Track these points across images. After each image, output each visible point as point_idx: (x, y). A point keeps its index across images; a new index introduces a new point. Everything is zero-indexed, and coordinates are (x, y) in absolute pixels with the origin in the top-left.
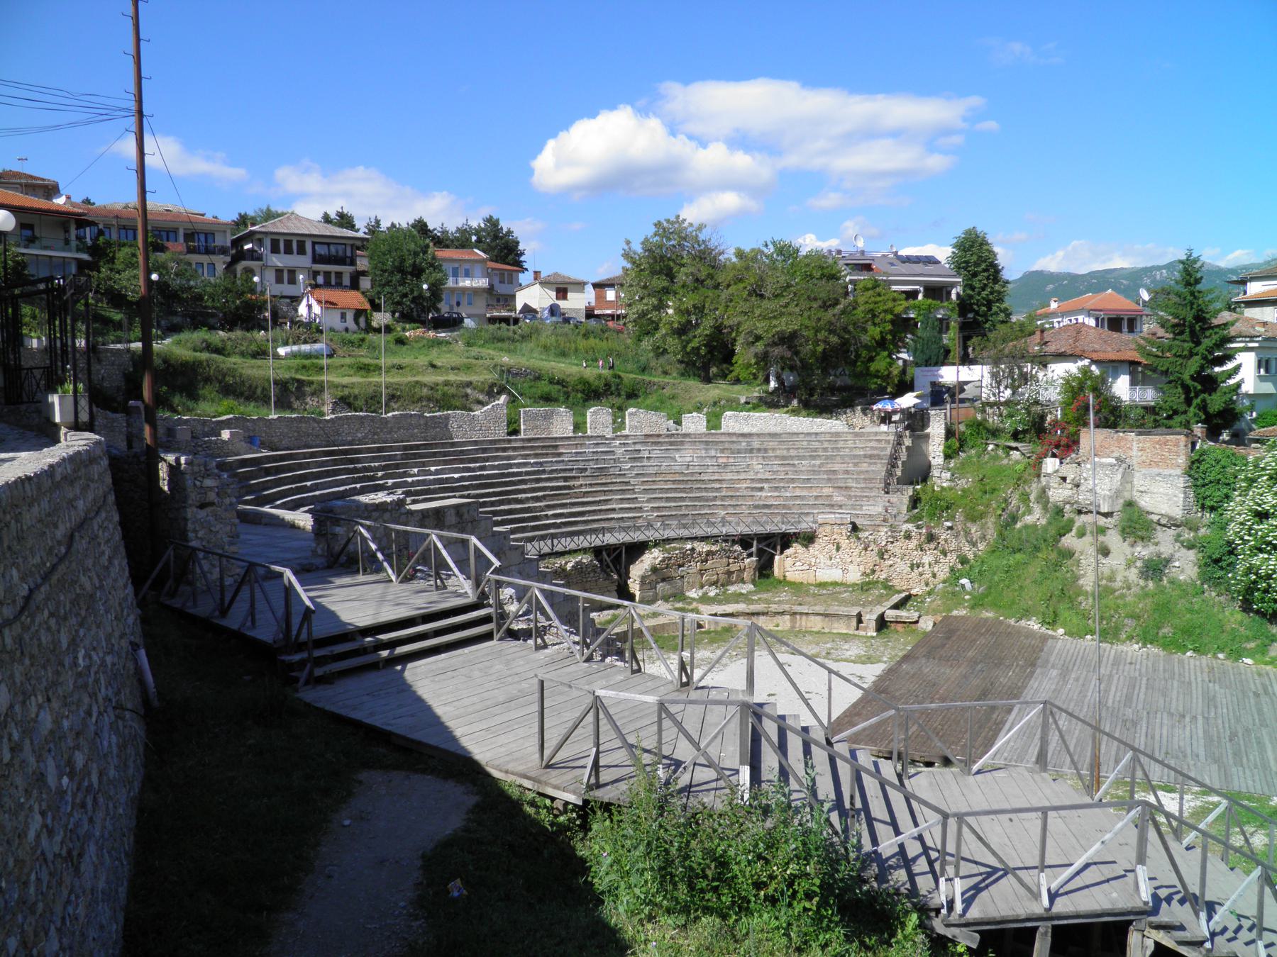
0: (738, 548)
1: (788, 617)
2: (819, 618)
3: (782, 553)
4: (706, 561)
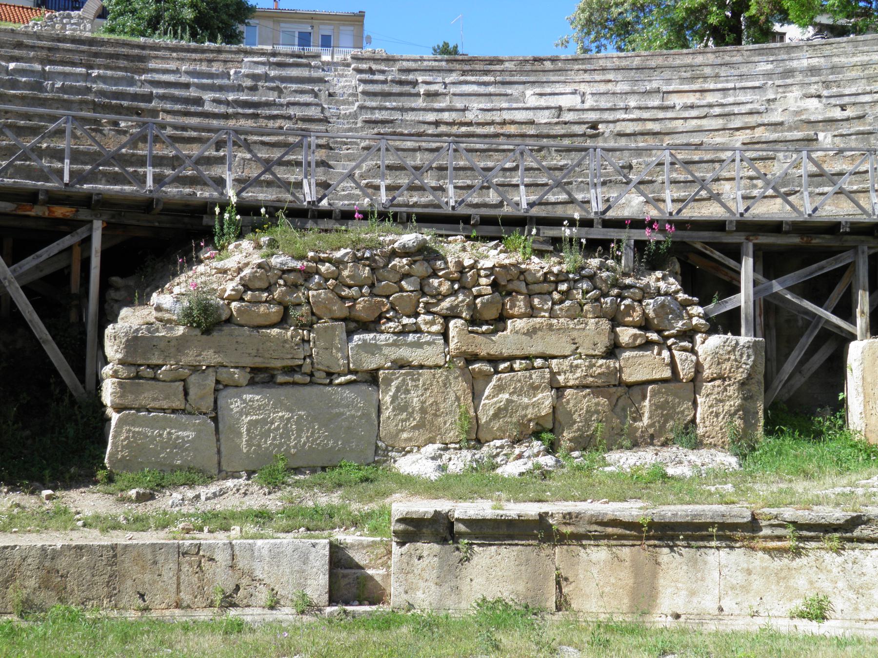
0: (664, 283)
4: (501, 320)
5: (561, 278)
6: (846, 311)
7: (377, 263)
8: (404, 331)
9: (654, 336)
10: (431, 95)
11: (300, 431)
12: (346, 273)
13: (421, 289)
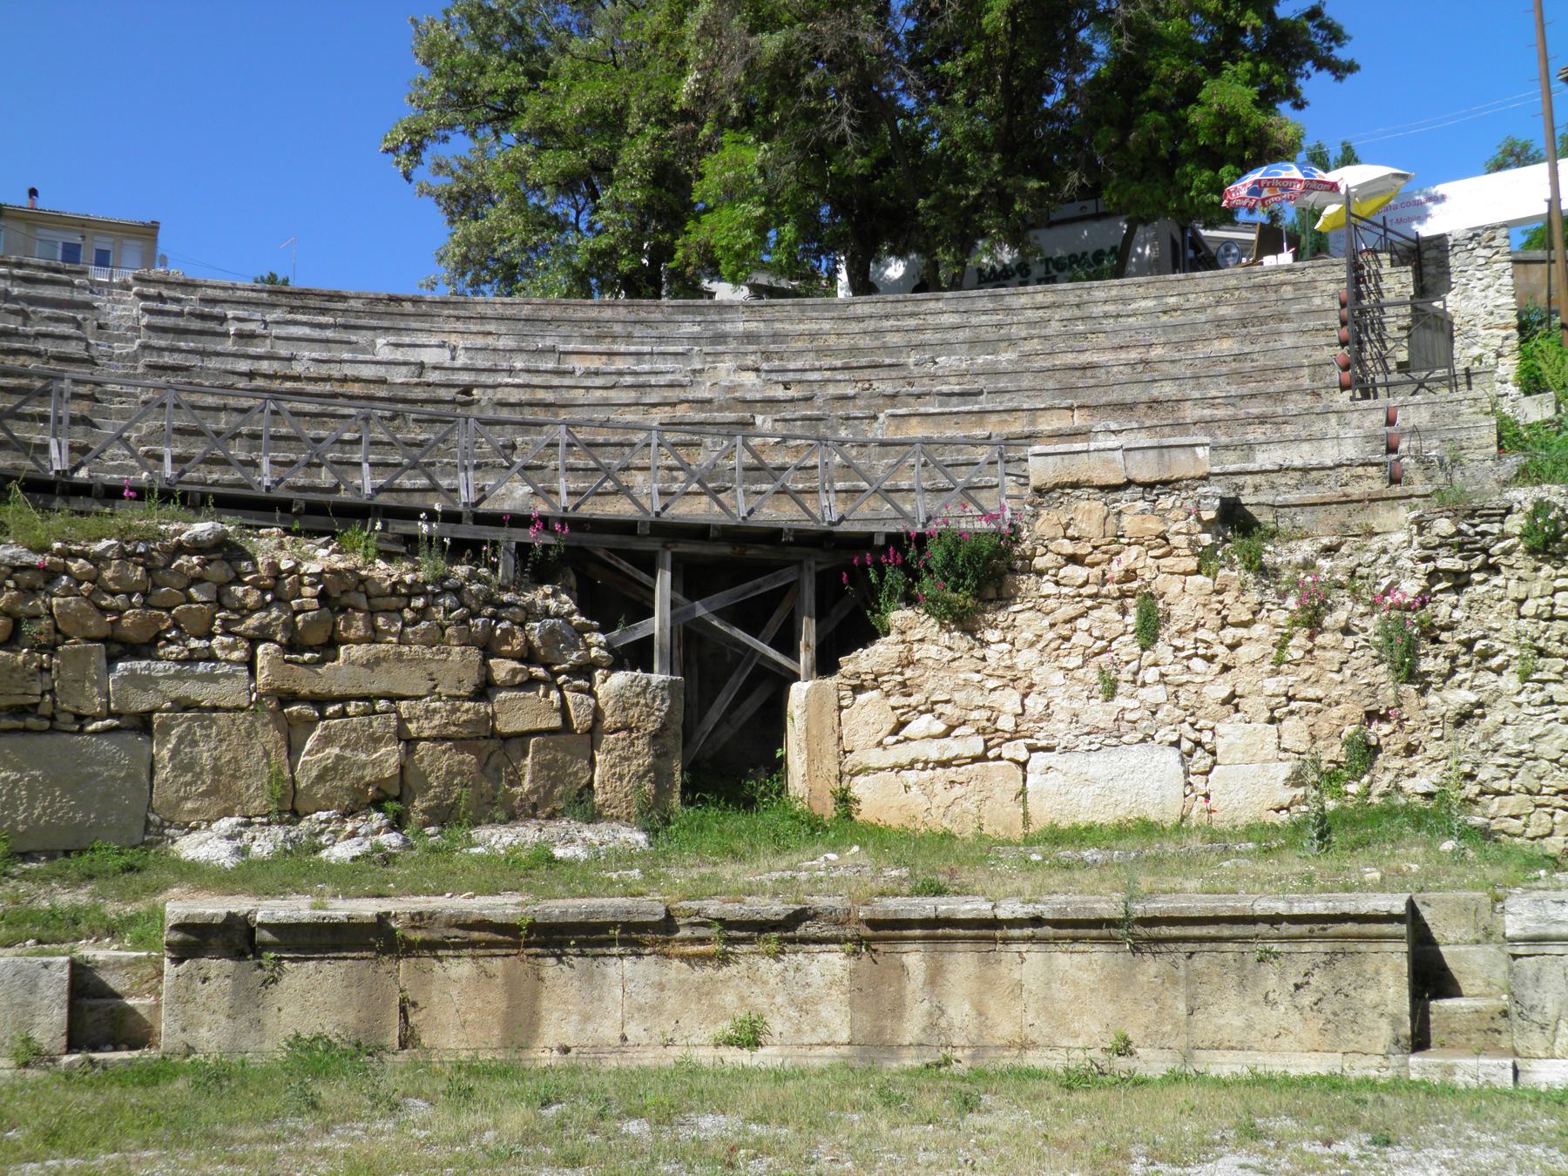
1: (832, 963)
2: (1083, 965)
3: (826, 665)
4: (329, 647)
5: (415, 590)
6: (787, 644)
7: (156, 563)
8: (192, 659)
9: (539, 672)
11: (32, 799)
12: (108, 574)
13: (219, 600)
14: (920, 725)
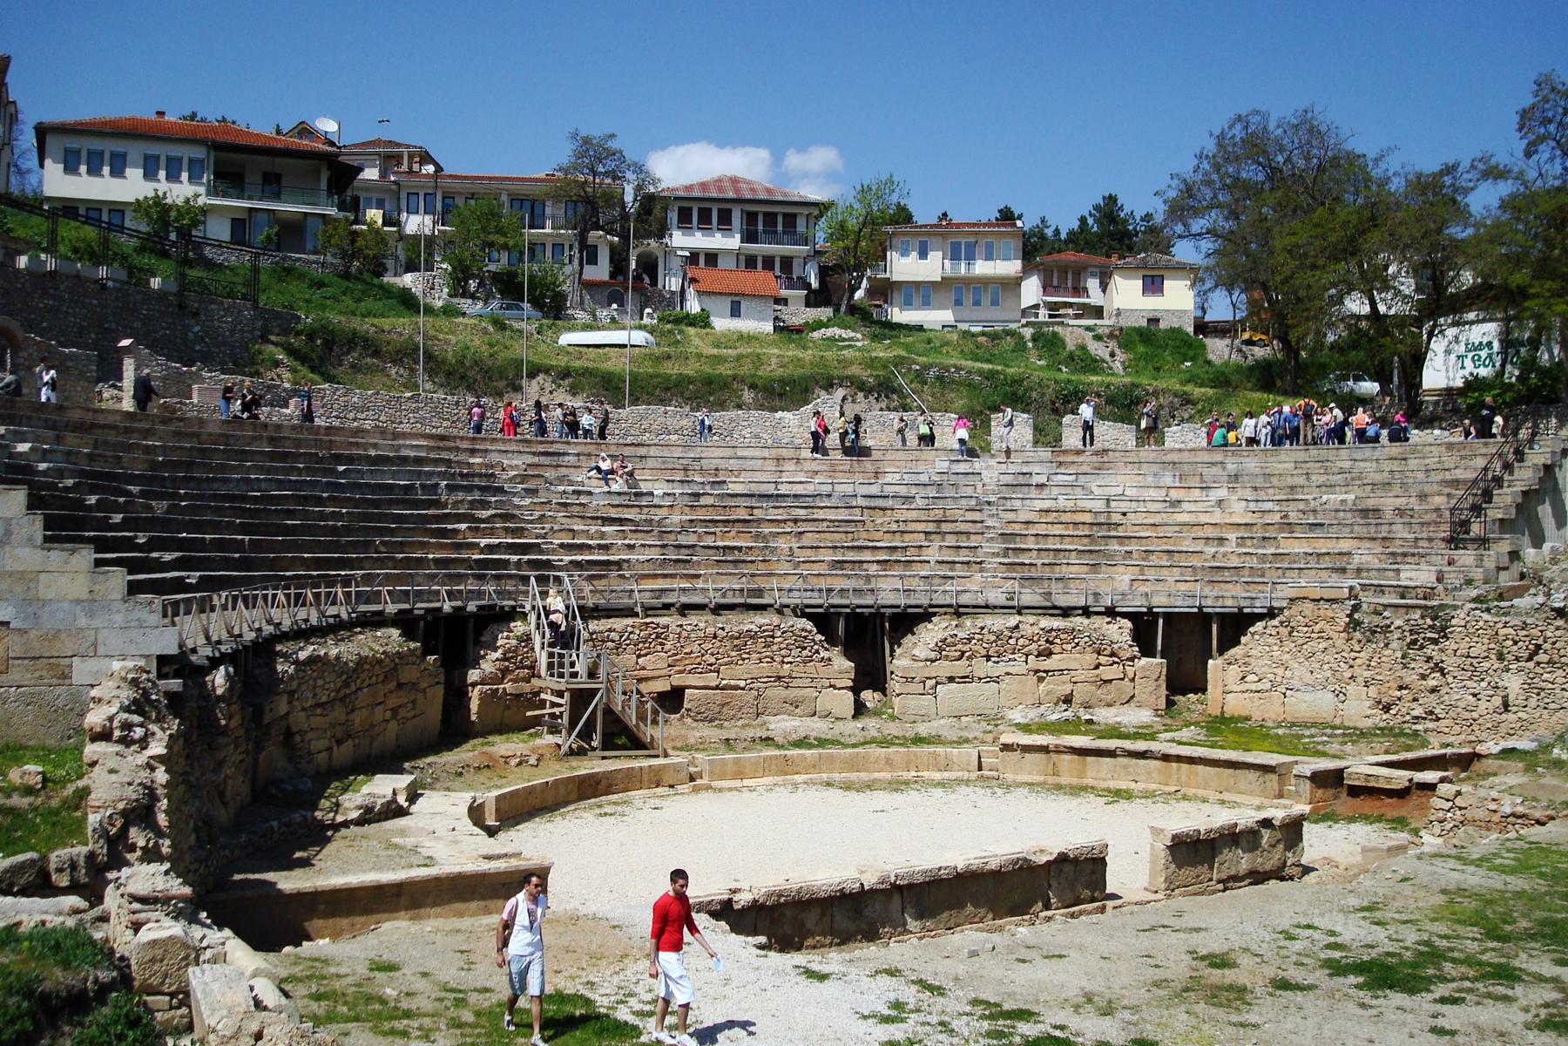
10: (1041, 486)
14: (1251, 678)
